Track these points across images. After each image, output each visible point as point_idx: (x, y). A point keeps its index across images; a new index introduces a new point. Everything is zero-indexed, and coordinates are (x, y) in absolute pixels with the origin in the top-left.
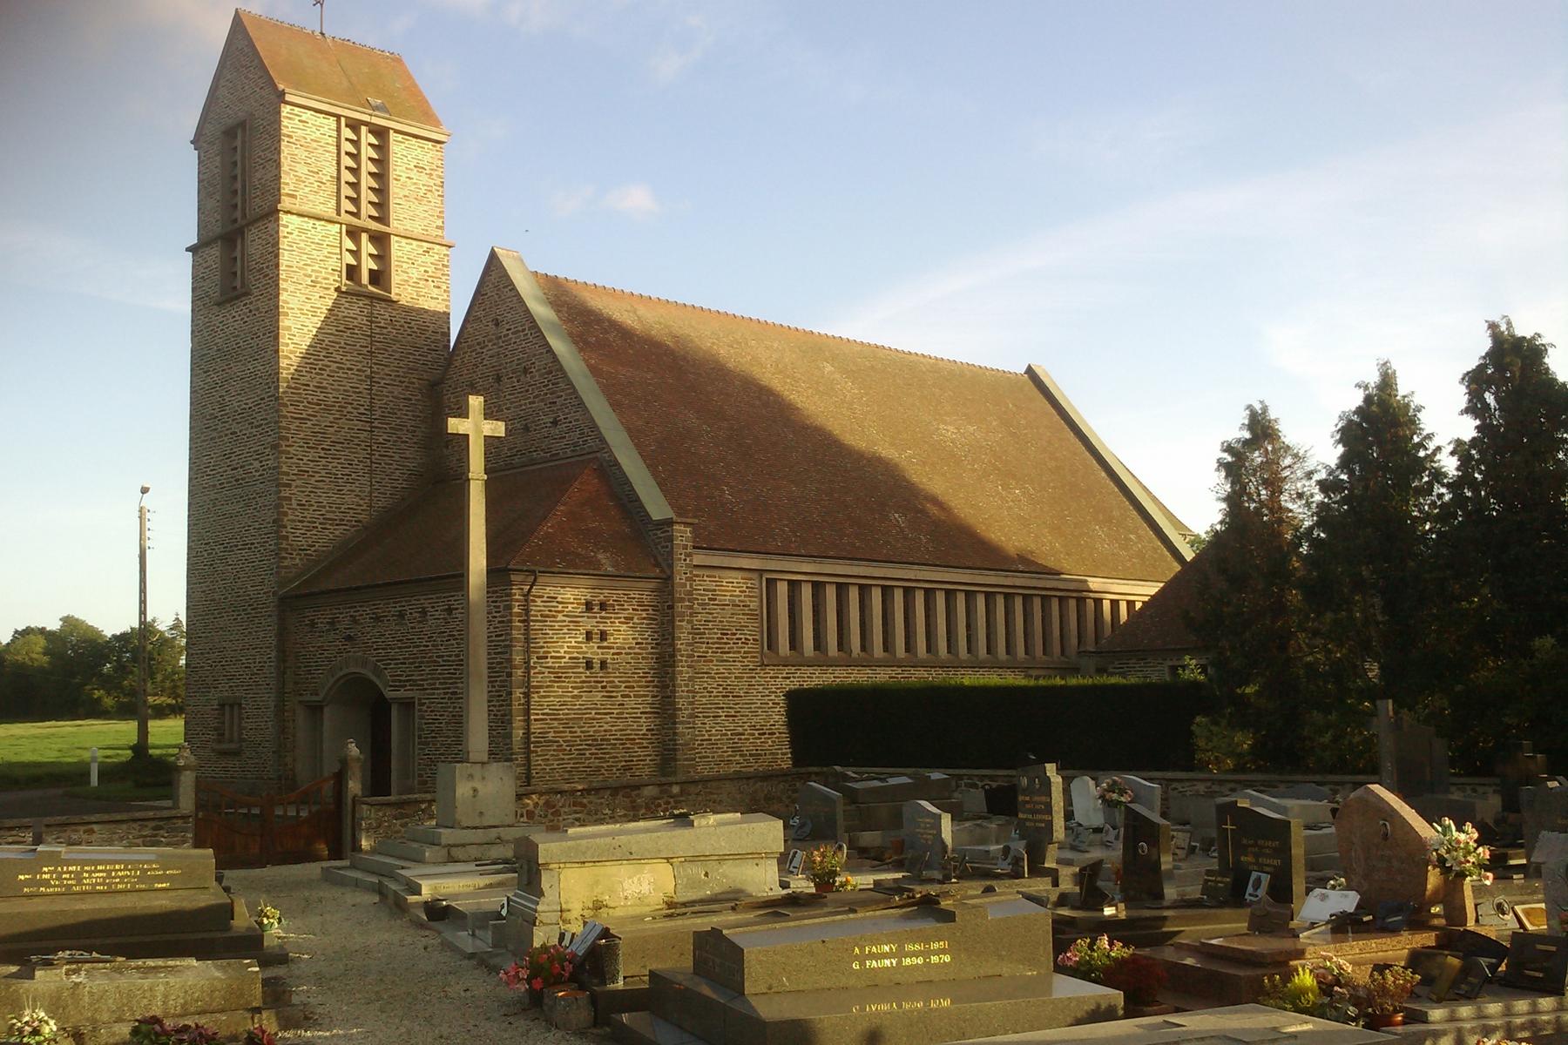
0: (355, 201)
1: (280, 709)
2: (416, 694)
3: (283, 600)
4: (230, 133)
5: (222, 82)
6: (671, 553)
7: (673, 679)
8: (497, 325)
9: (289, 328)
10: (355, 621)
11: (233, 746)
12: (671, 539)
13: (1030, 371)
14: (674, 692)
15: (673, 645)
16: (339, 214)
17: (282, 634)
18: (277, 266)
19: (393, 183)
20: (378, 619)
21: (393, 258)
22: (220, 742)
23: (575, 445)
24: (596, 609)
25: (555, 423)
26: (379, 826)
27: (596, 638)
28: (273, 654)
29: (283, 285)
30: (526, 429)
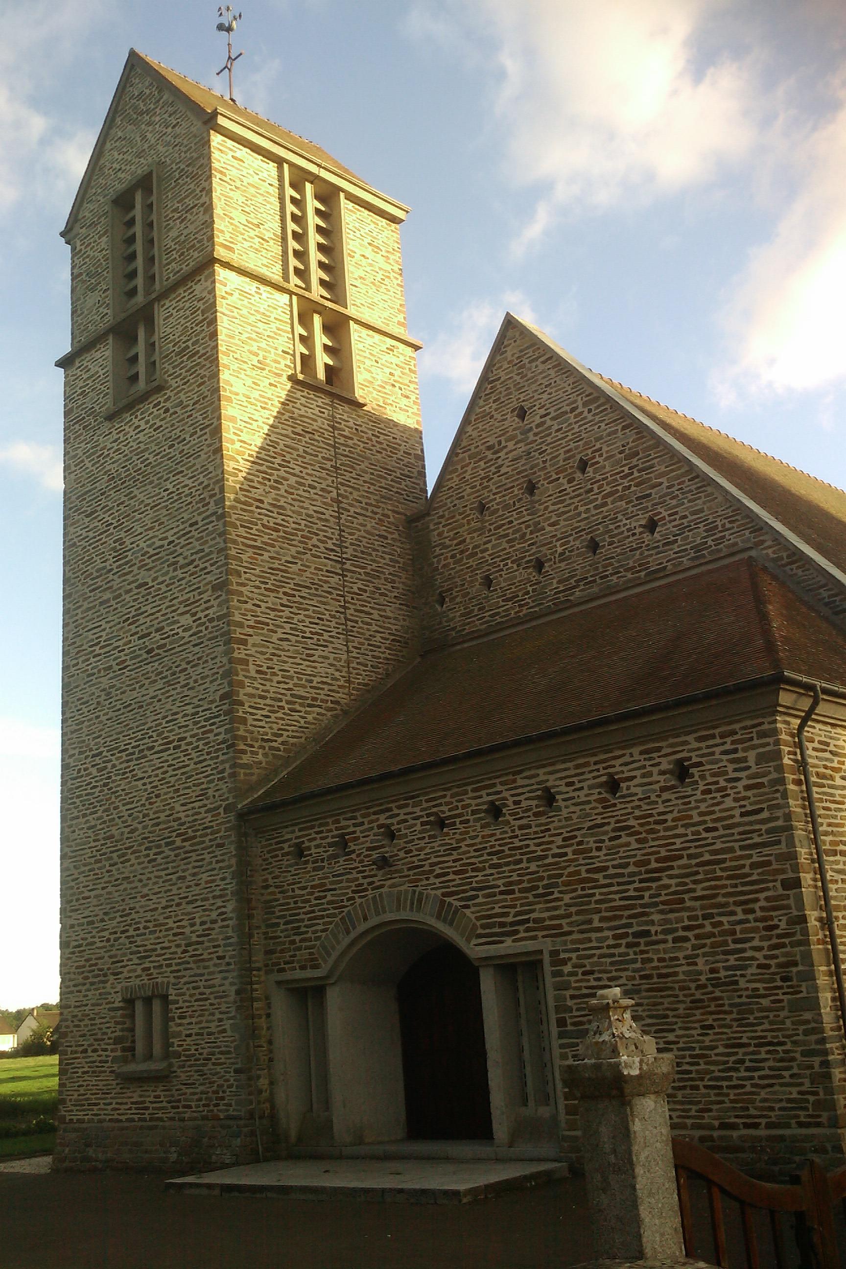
0: (302, 274)
1: (245, 996)
2: (546, 945)
3: (242, 816)
4: (123, 201)
5: (108, 146)
9: (233, 419)
10: (392, 835)
11: (152, 1066)
16: (286, 278)
17: (244, 874)
22: (125, 1061)
23: (697, 548)
25: (651, 526)
28: (230, 907)
29: (223, 359)
30: (594, 546)
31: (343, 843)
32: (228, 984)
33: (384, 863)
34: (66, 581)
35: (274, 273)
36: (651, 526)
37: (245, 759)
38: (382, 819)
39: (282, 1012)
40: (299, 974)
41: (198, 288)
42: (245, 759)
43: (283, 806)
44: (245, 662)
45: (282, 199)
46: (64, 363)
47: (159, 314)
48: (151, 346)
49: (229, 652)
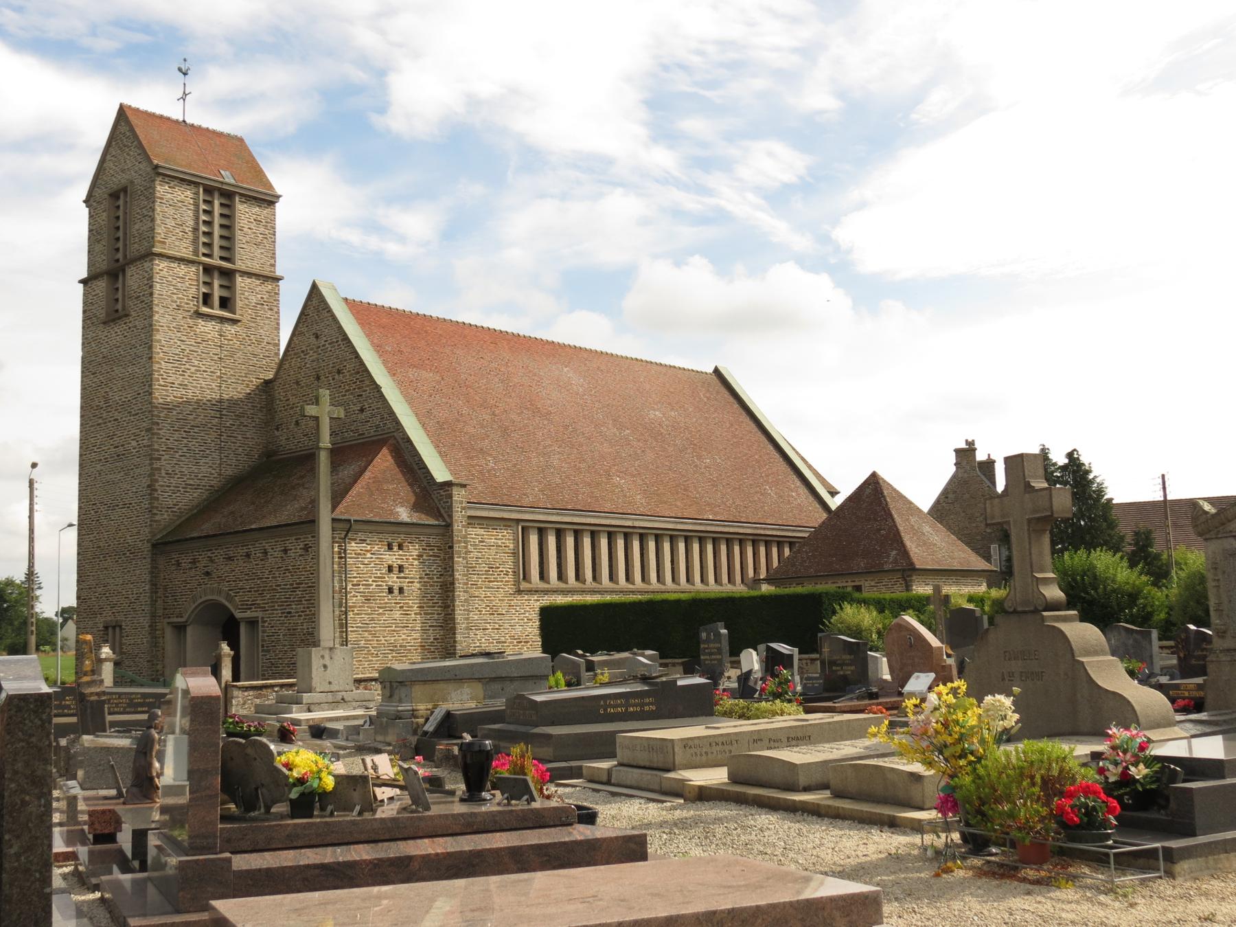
1: (153, 627)
2: (260, 614)
4: (115, 196)
5: (108, 157)
6: (451, 507)
7: (453, 601)
8: (317, 337)
9: (159, 341)
12: (451, 496)
13: (717, 371)
14: (453, 610)
15: (453, 575)
16: (196, 252)
17: (154, 572)
18: (151, 294)
19: (238, 233)
20: (230, 559)
21: (238, 288)
24: (395, 549)
25: (362, 410)
26: (244, 704)
27: (396, 570)
28: (147, 587)
29: (156, 309)
31: (194, 562)
32: (145, 622)
33: (207, 574)
34: (82, 408)
36: (362, 410)
37: (157, 518)
38: (209, 554)
39: (169, 634)
40: (175, 620)
41: (146, 265)
42: (157, 518)
43: (167, 544)
44: (159, 469)
45: (197, 211)
46: (84, 282)
47: (129, 272)
48: (124, 285)
49: (151, 464)
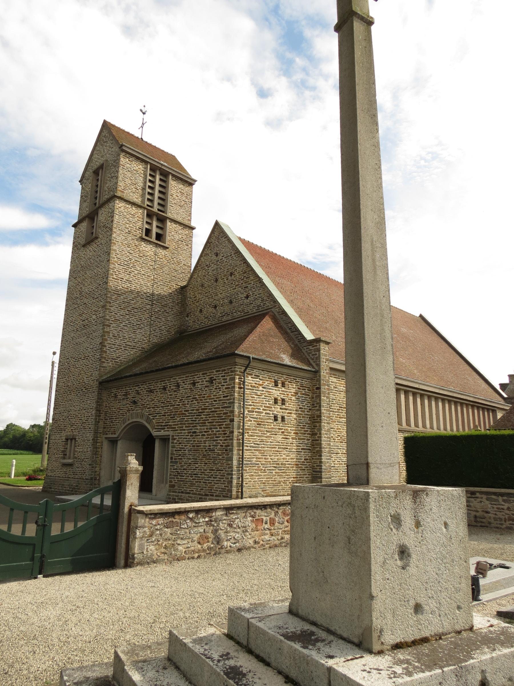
0: (151, 201)
1: (95, 441)
2: (171, 433)
3: (101, 383)
4: (96, 172)
5: (95, 153)
6: (319, 358)
7: (320, 430)
8: (217, 256)
9: (115, 250)
10: (138, 393)
11: (70, 461)
12: (319, 350)
13: (421, 316)
14: (320, 437)
15: (320, 410)
16: (143, 201)
17: (99, 402)
18: (112, 221)
19: (169, 197)
20: (151, 391)
21: (168, 228)
22: (64, 458)
23: (259, 306)
24: (280, 385)
25: (247, 297)
26: (151, 536)
27: (280, 402)
28: (94, 412)
29: (114, 230)
30: (231, 302)
31: (126, 394)
32: (90, 436)
33: (135, 402)
34: (67, 300)
35: (138, 201)
36: (247, 297)
37: (104, 365)
40: (111, 436)
42: (104, 365)
44: (109, 332)
45: (146, 176)
46: (75, 226)
49: (103, 329)
